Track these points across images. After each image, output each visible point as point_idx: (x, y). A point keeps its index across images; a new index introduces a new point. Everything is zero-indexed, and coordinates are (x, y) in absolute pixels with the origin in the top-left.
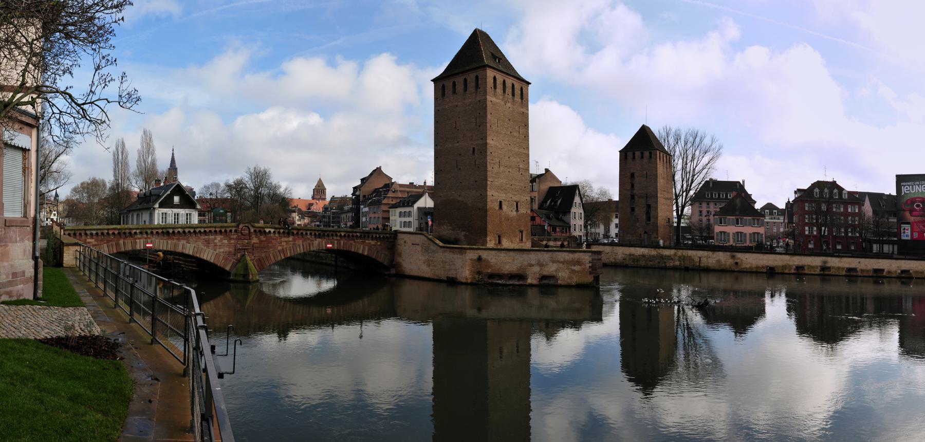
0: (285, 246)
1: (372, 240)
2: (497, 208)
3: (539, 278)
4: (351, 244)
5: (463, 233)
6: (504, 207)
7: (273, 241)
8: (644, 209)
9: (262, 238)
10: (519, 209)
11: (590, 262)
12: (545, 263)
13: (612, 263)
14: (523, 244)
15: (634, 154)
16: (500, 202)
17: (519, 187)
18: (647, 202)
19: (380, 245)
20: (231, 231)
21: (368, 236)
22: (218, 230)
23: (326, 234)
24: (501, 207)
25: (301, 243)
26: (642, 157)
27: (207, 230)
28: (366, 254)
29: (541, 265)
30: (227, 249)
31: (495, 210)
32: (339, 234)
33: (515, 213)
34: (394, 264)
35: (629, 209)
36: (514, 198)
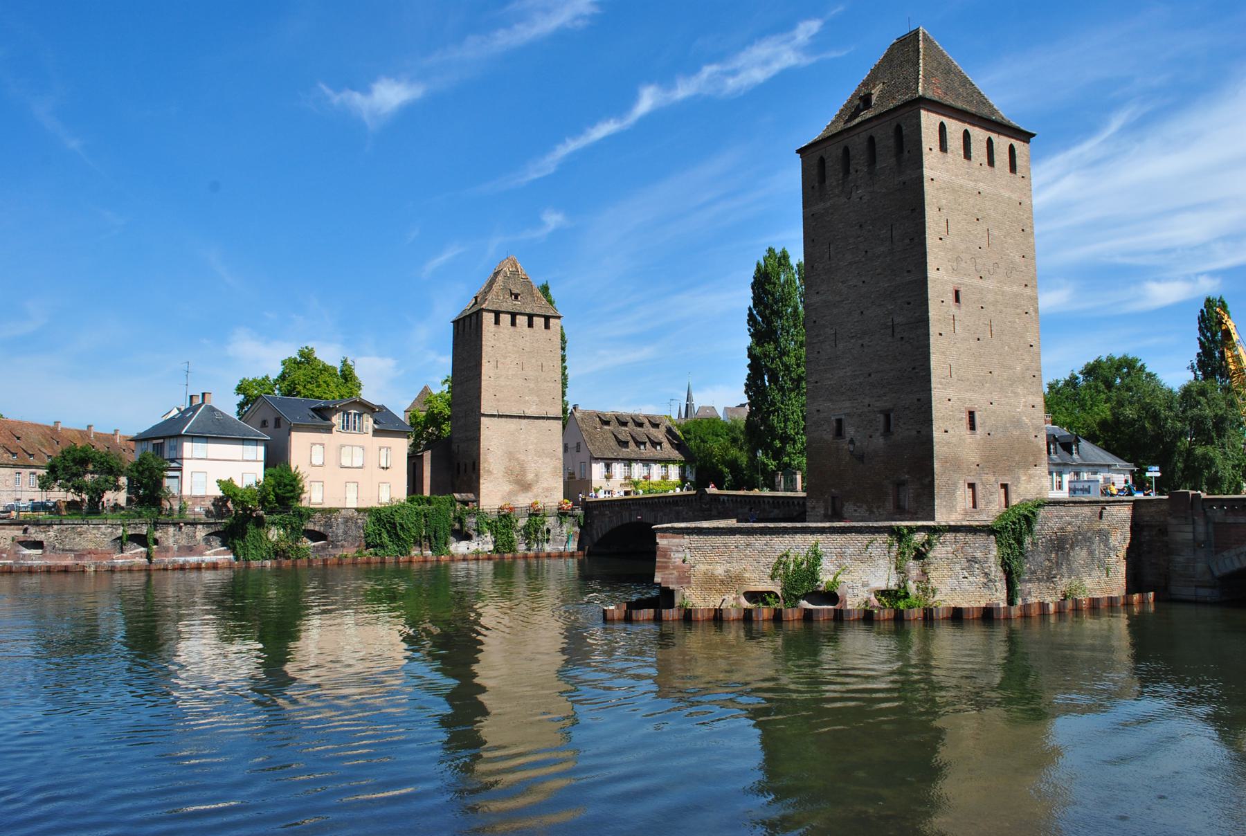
2: (829, 436)
6: (850, 431)
10: (892, 429)
16: (839, 421)
24: (839, 432)
32: (796, 503)
33: (881, 440)
36: (878, 404)
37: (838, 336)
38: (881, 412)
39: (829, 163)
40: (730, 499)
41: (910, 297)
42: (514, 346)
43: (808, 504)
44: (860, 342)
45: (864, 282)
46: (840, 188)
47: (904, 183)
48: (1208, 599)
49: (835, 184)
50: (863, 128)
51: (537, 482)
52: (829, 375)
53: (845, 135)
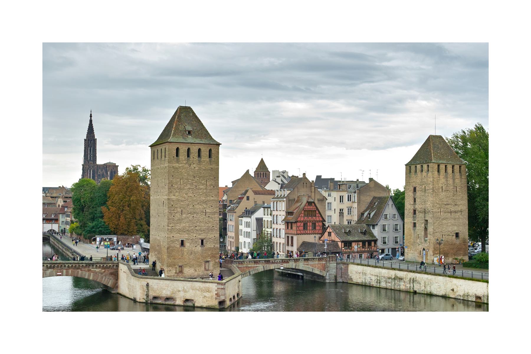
2: (178, 246)
3: (183, 301)
4: (78, 272)
5: (159, 263)
6: (187, 244)
8: (423, 225)
10: (204, 245)
11: (216, 291)
12: (187, 290)
13: (362, 283)
15: (416, 166)
16: (182, 242)
18: (425, 217)
21: (93, 266)
23: (56, 265)
26: (422, 172)
28: (91, 278)
29: (185, 291)
31: (177, 248)
33: (200, 248)
34: (116, 285)
35: (412, 225)
36: (199, 236)
37: (183, 212)
38: (200, 239)
39: (181, 151)
41: (212, 204)
44: (192, 215)
45: (195, 196)
46: (186, 161)
47: (212, 168)
49: (184, 159)
50: (197, 145)
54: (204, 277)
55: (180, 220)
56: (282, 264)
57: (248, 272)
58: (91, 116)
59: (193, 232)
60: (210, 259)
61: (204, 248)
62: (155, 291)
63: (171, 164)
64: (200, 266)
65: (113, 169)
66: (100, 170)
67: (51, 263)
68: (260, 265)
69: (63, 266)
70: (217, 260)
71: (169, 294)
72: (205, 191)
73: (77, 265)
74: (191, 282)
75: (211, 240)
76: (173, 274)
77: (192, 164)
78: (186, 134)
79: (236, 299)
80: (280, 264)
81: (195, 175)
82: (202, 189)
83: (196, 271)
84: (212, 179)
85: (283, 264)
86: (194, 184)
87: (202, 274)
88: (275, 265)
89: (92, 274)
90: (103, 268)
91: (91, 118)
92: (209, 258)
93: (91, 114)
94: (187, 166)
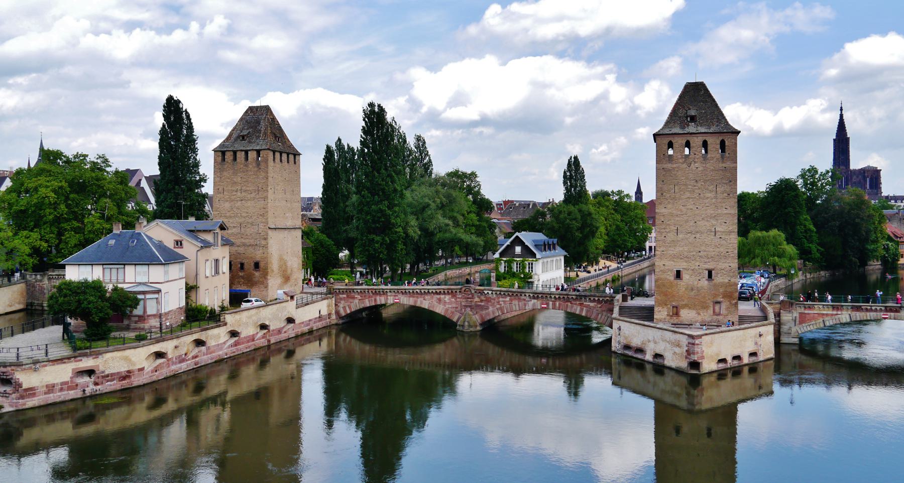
0: (503, 305)
1: (590, 302)
2: (672, 278)
4: (567, 305)
6: (685, 276)
7: (492, 300)
9: (483, 298)
11: (687, 346)
12: (657, 341)
14: (720, 318)
17: (714, 253)
19: (600, 307)
20: (456, 292)
22: (446, 291)
23: (540, 296)
25: (517, 303)
27: (438, 291)
28: (584, 314)
30: (454, 305)
31: (668, 280)
32: (553, 296)
33: (706, 282)
36: (704, 266)
38: (706, 269)
40: (494, 293)
42: (281, 176)
43: (656, 309)
46: (683, 160)
47: (725, 168)
48: (797, 342)
49: (680, 157)
51: (291, 274)
52: (672, 249)
53: (689, 135)
54: (713, 324)
55: (674, 243)
56: (885, 313)
57: (821, 320)
58: (841, 110)
59: (695, 260)
60: (722, 299)
61: (712, 282)
62: (626, 338)
63: (660, 165)
64: (705, 307)
65: (874, 174)
66: (855, 177)
67: (533, 293)
68: (843, 312)
69: (549, 296)
70: (734, 302)
71: (639, 344)
72: (714, 200)
73: (565, 296)
74: (661, 330)
75: (722, 271)
76: (663, 317)
77: (693, 163)
78: (687, 120)
79: (746, 360)
80: (882, 313)
81: (697, 179)
82: (707, 198)
83: (699, 314)
84: (726, 184)
85: (889, 313)
86: (696, 191)
87: (709, 319)
88: (872, 314)
89: (585, 308)
90: (599, 302)
91: (841, 112)
92: (720, 297)
93: (841, 108)
94: (685, 166)
